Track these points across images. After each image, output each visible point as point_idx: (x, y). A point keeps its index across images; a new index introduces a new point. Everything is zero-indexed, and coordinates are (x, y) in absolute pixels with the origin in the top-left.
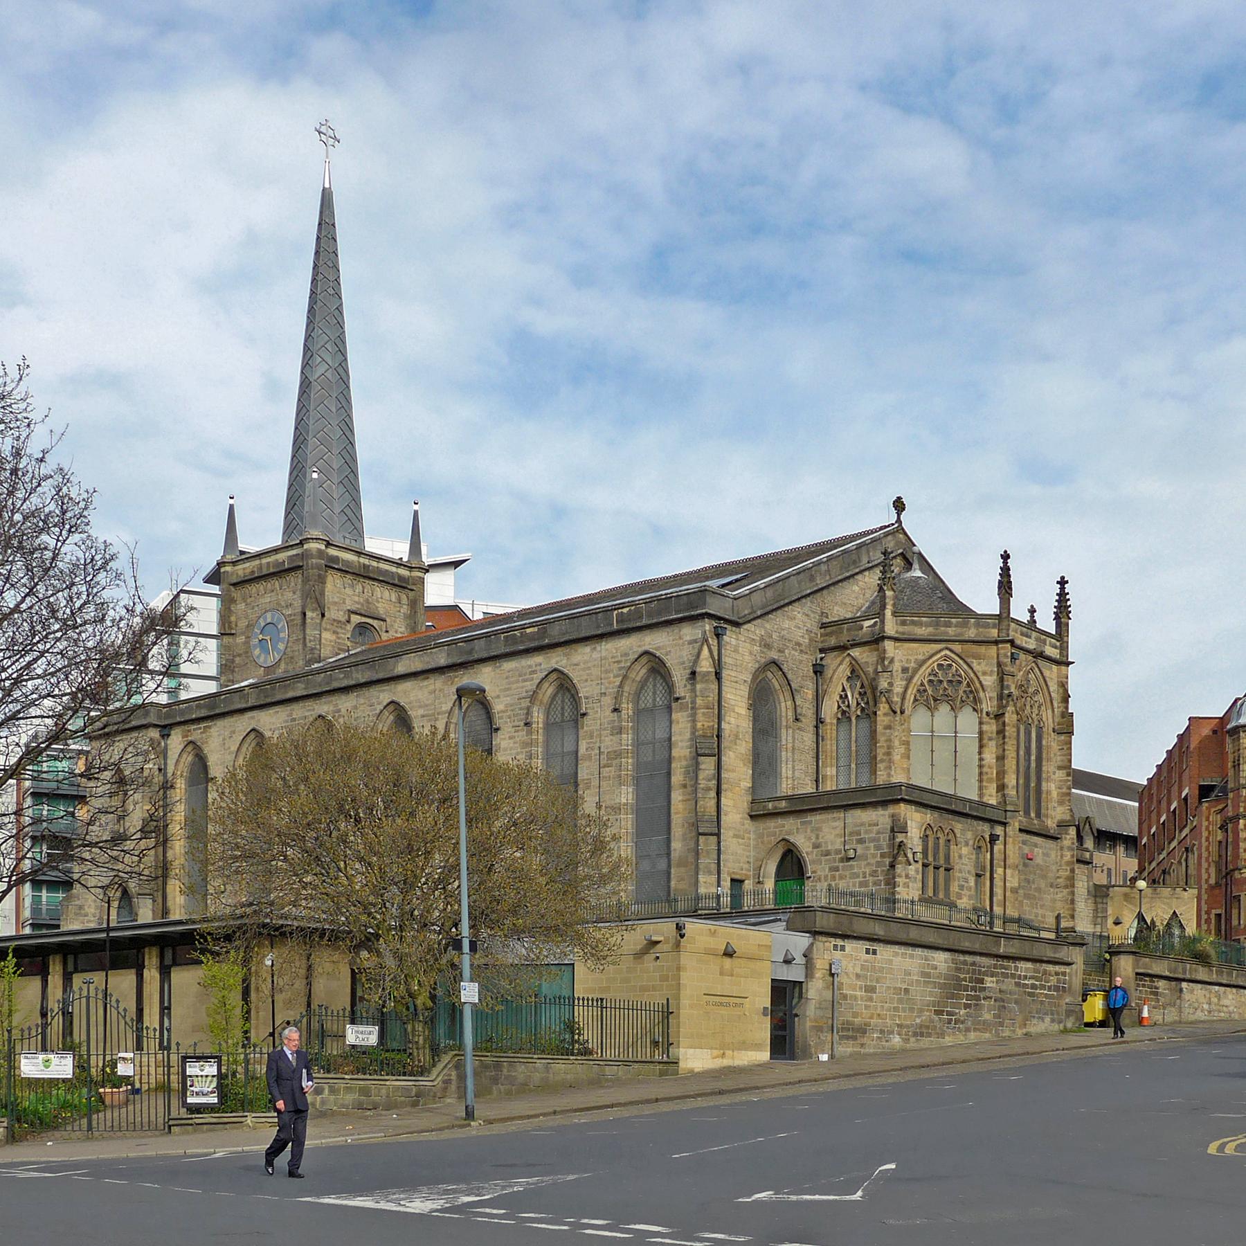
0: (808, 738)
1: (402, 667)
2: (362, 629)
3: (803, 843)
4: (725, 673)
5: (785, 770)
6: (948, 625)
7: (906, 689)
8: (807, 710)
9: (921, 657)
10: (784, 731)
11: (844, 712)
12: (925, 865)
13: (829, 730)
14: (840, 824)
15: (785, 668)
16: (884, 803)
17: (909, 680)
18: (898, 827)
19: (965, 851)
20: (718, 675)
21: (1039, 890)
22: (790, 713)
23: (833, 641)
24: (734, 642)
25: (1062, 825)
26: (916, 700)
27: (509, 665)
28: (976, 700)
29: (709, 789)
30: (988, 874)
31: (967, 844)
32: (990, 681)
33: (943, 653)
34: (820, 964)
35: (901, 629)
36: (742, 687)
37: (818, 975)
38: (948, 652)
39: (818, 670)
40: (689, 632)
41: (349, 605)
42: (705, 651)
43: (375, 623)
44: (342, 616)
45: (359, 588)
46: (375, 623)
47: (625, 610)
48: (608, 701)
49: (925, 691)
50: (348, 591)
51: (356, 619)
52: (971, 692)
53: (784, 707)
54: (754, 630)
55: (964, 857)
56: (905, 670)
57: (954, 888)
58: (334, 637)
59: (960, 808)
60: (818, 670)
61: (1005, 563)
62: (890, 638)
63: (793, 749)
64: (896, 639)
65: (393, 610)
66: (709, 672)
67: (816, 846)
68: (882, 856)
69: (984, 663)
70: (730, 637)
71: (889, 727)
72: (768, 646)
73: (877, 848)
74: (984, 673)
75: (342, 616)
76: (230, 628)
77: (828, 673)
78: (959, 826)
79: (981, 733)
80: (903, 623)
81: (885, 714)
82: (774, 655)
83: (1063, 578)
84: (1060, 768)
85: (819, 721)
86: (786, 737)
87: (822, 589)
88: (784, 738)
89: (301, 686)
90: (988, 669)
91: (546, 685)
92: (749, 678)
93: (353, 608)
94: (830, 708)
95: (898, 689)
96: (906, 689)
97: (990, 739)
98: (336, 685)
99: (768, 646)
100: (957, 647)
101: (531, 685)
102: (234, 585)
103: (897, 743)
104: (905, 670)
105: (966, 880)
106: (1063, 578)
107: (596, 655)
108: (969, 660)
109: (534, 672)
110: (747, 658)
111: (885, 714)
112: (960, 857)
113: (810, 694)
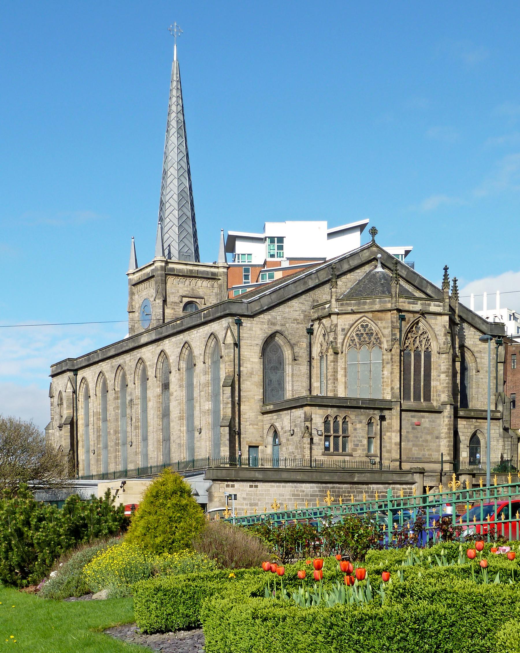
0: (304, 368)
1: (144, 339)
3: (278, 425)
4: (242, 343)
5: (288, 387)
6: (365, 304)
8: (303, 353)
9: (352, 322)
10: (287, 366)
13: (315, 363)
14: (288, 417)
15: (286, 333)
16: (302, 406)
18: (309, 419)
19: (358, 426)
20: (237, 345)
21: (426, 441)
22: (290, 357)
24: (249, 325)
25: (444, 404)
26: (350, 345)
27: (173, 339)
28: (380, 343)
29: (228, 403)
30: (379, 437)
31: (360, 422)
33: (362, 319)
36: (255, 348)
38: (365, 318)
40: (225, 322)
41: (182, 292)
44: (177, 300)
45: (187, 282)
48: (202, 357)
49: (354, 340)
52: (378, 338)
53: (288, 354)
54: (265, 317)
56: (343, 330)
57: (350, 446)
58: (173, 311)
59: (354, 404)
60: (310, 332)
63: (293, 375)
64: (338, 314)
65: (208, 291)
66: (230, 343)
67: (282, 429)
69: (384, 322)
72: (274, 324)
74: (384, 328)
75: (177, 300)
76: (132, 308)
78: (352, 415)
80: (342, 305)
81: (331, 355)
82: (278, 328)
83: (446, 266)
85: (311, 359)
86: (288, 369)
88: (287, 370)
89: (113, 349)
90: (386, 325)
94: (316, 351)
97: (388, 363)
98: (124, 349)
99: (274, 324)
100: (370, 315)
102: (134, 285)
103: (339, 369)
104: (343, 330)
105: (361, 441)
106: (446, 266)
108: (376, 322)
110: (259, 332)
111: (331, 355)
112: (355, 429)
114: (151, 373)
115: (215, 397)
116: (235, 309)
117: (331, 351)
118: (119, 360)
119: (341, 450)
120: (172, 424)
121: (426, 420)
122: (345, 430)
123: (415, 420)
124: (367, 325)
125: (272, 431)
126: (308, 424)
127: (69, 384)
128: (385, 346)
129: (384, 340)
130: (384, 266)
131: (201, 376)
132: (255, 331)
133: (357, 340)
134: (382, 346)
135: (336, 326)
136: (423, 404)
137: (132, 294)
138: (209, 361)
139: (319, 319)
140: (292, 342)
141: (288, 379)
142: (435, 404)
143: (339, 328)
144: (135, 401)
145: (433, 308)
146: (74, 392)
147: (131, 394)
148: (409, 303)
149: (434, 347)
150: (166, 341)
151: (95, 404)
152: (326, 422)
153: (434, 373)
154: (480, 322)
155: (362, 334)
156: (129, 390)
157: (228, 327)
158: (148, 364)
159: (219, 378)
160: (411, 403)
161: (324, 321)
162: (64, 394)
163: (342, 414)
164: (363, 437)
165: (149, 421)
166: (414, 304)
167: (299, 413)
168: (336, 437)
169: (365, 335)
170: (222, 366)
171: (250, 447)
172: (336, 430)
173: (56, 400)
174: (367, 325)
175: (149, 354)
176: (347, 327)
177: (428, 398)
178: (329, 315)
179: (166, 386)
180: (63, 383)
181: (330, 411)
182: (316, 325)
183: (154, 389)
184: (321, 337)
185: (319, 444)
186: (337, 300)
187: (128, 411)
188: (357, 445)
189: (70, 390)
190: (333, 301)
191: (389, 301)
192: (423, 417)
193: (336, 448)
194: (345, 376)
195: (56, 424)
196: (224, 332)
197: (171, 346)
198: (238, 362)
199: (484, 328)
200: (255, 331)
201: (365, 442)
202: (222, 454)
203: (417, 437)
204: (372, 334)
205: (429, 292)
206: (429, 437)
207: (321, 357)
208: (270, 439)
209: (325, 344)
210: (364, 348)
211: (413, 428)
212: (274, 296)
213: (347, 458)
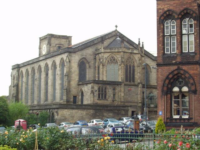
2: (59, 47)
5: (87, 76)
12: (99, 94)
16: (91, 83)
17: (106, 60)
19: (110, 90)
23: (97, 53)
25: (139, 83)
31: (110, 89)
32: (120, 59)
42: (67, 58)
43: (61, 46)
44: (54, 45)
46: (61, 46)
48: (59, 66)
50: (56, 41)
51: (57, 45)
53: (87, 65)
54: (79, 53)
55: (110, 91)
56: (105, 58)
57: (107, 97)
58: (53, 49)
60: (95, 59)
62: (102, 53)
67: (84, 90)
70: (73, 55)
78: (108, 87)
79: (119, 68)
80: (105, 50)
86: (87, 71)
87: (96, 44)
92: (78, 61)
93: (57, 43)
100: (114, 53)
103: (104, 71)
104: (105, 58)
112: (109, 91)
113: (93, 63)
114: (43, 70)
115: (62, 79)
116: (70, 50)
117: (101, 65)
118: (33, 65)
119: (104, 98)
120: (49, 88)
121: (133, 89)
122: (105, 92)
123: (129, 88)
124: (113, 57)
125: (81, 92)
127: (17, 73)
128: (119, 64)
129: (118, 62)
130: (120, 37)
131: (58, 71)
132: (76, 58)
133: (110, 61)
135: (103, 56)
136: (132, 83)
137: (40, 43)
138: (61, 67)
139: (98, 54)
140: (89, 61)
141: (87, 73)
142: (136, 83)
143: (104, 57)
144: (37, 79)
145: (135, 52)
146: (18, 75)
147: (36, 77)
148: (127, 50)
149: (136, 65)
150: (48, 60)
151: (24, 79)
152: (99, 89)
153: (136, 73)
154: (151, 56)
156: (35, 75)
157: (67, 56)
158: (42, 67)
159: (64, 73)
160: (128, 83)
162: (15, 76)
163: (104, 86)
164: (111, 94)
165: (42, 85)
166: (129, 50)
167: (90, 86)
168: (102, 94)
170: (65, 69)
171: (74, 96)
172: (102, 92)
173: (13, 77)
174: (113, 57)
175: (42, 64)
176: (107, 57)
177: (134, 81)
178: (101, 53)
179: (47, 75)
180: (15, 71)
181: (100, 85)
182: (97, 56)
183: (43, 76)
184: (99, 61)
185: (96, 96)
186: (104, 48)
187: (35, 82)
188: (109, 97)
189: (17, 74)
190: (102, 48)
191: (121, 49)
192: (132, 87)
193: (102, 98)
194: (106, 73)
195: (12, 85)
196: (66, 57)
197: (50, 62)
198: (70, 68)
199: (153, 58)
200: (76, 58)
201: (112, 95)
202: (64, 99)
203: (130, 94)
204: (115, 60)
205: (135, 46)
206: (134, 94)
208: (80, 94)
209: (99, 63)
210: (113, 64)
211: (129, 91)
212: (83, 46)
213: (106, 101)
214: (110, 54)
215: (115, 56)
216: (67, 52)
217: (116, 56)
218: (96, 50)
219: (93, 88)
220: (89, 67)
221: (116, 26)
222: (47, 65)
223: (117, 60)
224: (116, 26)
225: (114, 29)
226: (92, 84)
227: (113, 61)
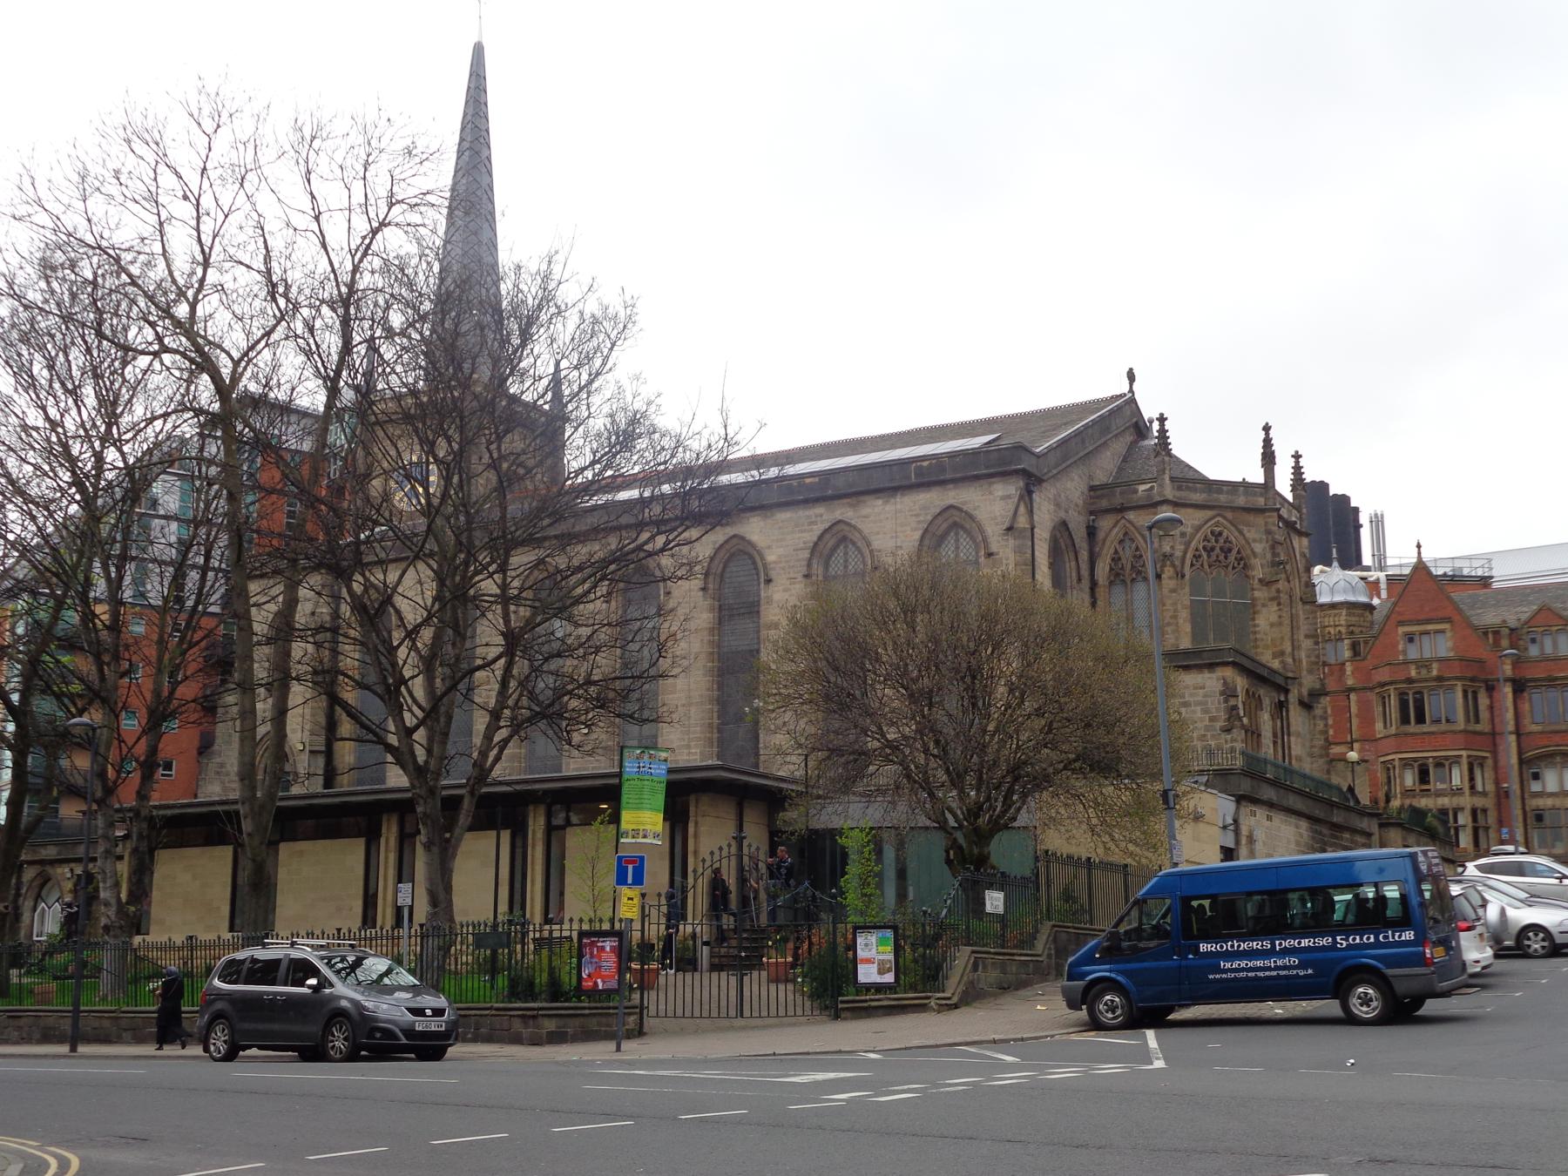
7: (1185, 553)
11: (1118, 575)
13: (1101, 592)
16: (1211, 666)
17: (1188, 544)
27: (783, 516)
34: (1244, 831)
35: (1178, 494)
37: (1244, 841)
39: (1091, 532)
47: (925, 464)
60: (1091, 532)
61: (1267, 434)
68: (1212, 719)
71: (1173, 591)
73: (1205, 711)
74: (1255, 541)
77: (1101, 535)
80: (1180, 488)
84: (1307, 636)
90: (1257, 536)
91: (828, 536)
95: (1178, 554)
96: (1185, 553)
97: (1264, 605)
100: (1229, 515)
101: (811, 537)
107: (888, 508)
109: (814, 523)
124: (1220, 534)
126: (1232, 702)
129: (1256, 562)
133: (1204, 555)
134: (1250, 573)
139: (1122, 509)
155: (1213, 549)
161: (1131, 515)
169: (1217, 550)
174: (1220, 534)
182: (1105, 523)
186: (1172, 479)
204: (1230, 550)
207: (1111, 583)
214: (1210, 513)
215: (1234, 536)
216: (1004, 474)
217: (1241, 533)
218: (1092, 488)
219: (1228, 693)
220: (1079, 580)
221: (1131, 376)
222: (741, 553)
223: (1246, 552)
224: (1131, 376)
225: (1124, 387)
226: (1228, 672)
227: (1222, 558)
